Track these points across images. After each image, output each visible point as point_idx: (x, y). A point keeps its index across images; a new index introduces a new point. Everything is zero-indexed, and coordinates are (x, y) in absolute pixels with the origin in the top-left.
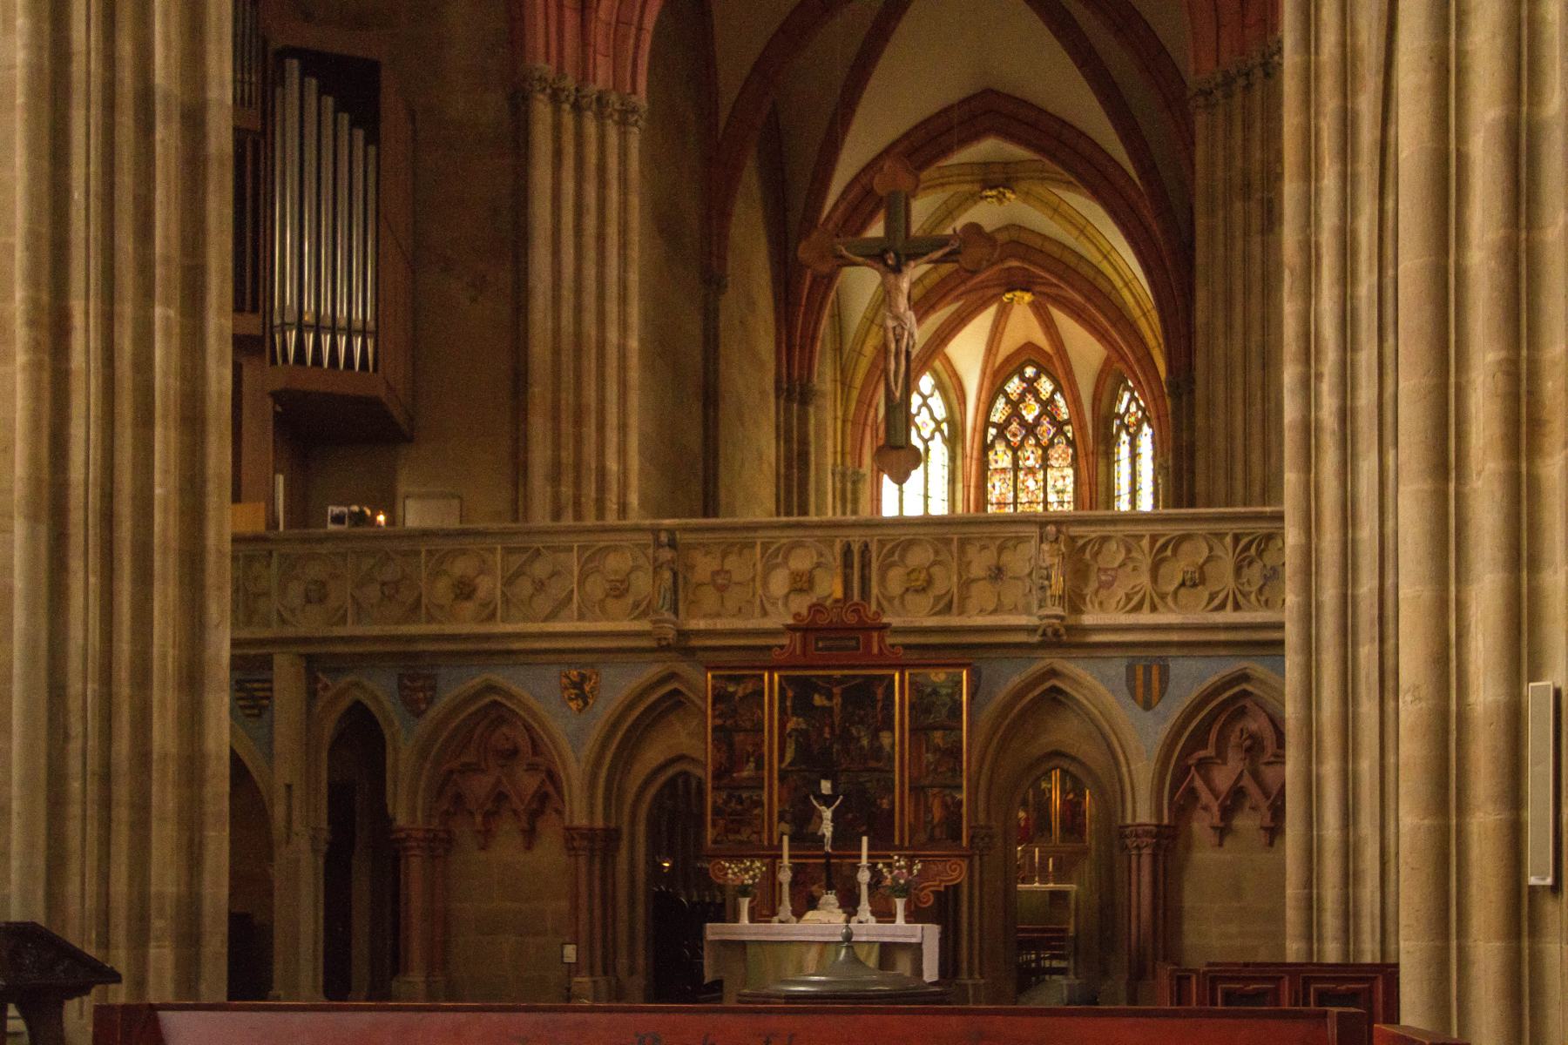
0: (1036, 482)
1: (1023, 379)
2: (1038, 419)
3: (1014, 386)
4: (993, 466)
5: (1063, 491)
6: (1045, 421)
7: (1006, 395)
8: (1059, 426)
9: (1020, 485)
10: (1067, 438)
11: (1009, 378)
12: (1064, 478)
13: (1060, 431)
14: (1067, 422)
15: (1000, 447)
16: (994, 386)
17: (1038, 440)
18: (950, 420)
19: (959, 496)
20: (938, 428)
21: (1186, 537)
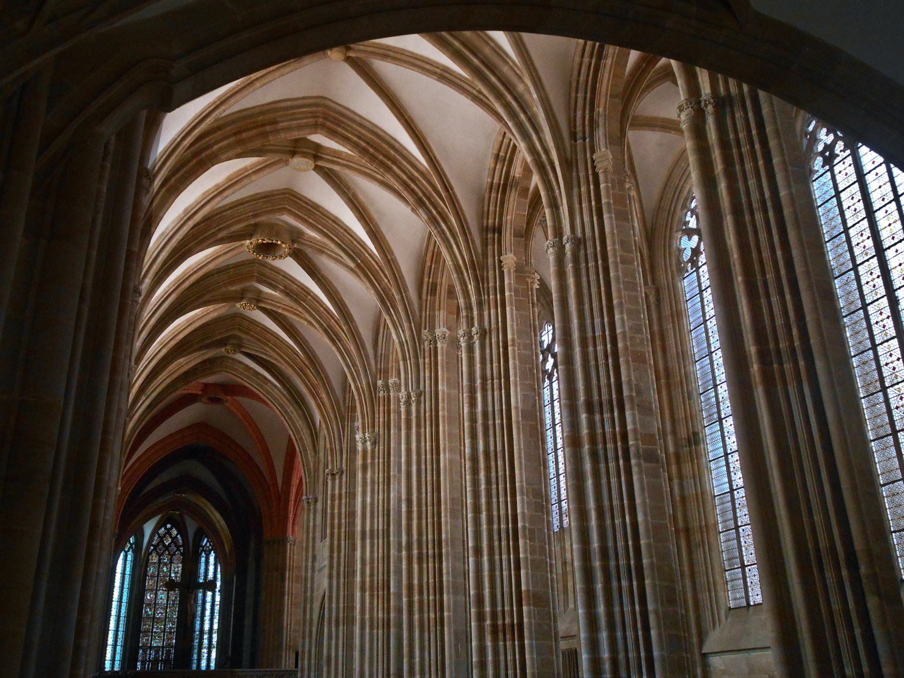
0: (167, 568)
1: (166, 528)
2: (170, 544)
3: (162, 531)
4: (151, 561)
5: (177, 573)
6: (173, 545)
7: (159, 534)
8: (178, 547)
9: (160, 570)
10: (181, 552)
11: (160, 528)
12: (178, 567)
13: (178, 550)
14: (181, 546)
15: (154, 555)
16: (155, 531)
17: (169, 552)
18: (136, 543)
19: (137, 574)
20: (131, 547)
21: (265, 675)
